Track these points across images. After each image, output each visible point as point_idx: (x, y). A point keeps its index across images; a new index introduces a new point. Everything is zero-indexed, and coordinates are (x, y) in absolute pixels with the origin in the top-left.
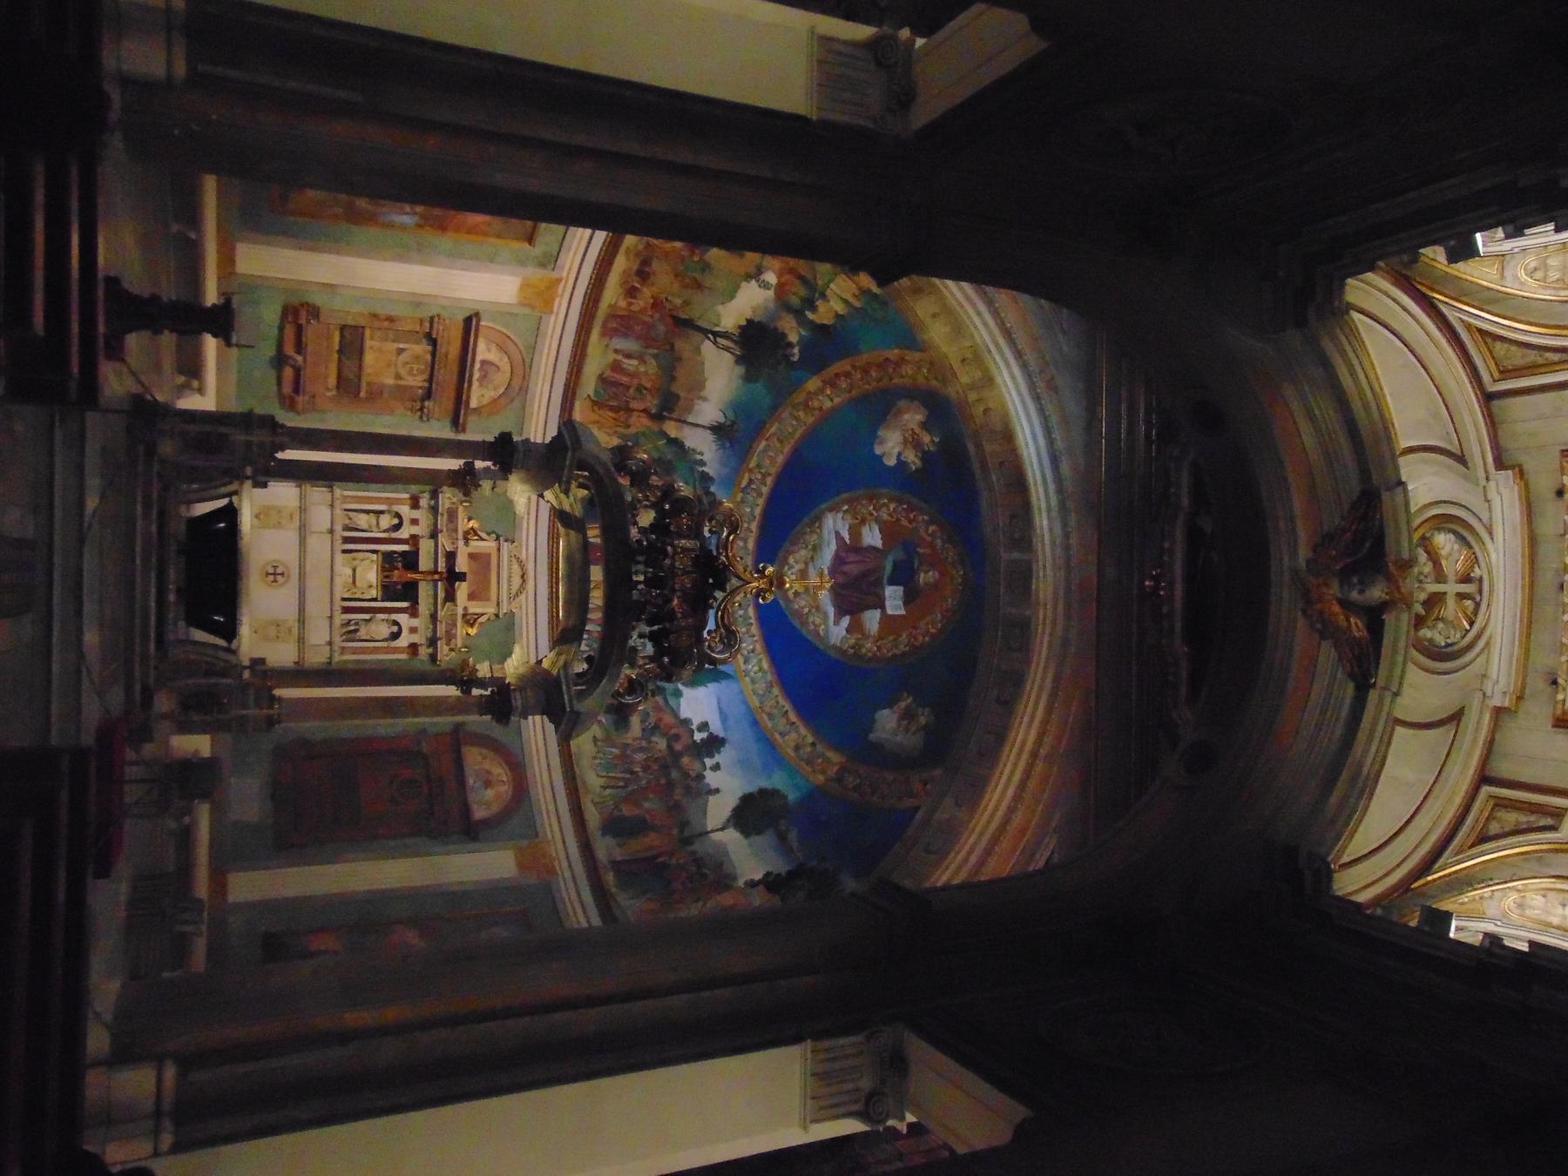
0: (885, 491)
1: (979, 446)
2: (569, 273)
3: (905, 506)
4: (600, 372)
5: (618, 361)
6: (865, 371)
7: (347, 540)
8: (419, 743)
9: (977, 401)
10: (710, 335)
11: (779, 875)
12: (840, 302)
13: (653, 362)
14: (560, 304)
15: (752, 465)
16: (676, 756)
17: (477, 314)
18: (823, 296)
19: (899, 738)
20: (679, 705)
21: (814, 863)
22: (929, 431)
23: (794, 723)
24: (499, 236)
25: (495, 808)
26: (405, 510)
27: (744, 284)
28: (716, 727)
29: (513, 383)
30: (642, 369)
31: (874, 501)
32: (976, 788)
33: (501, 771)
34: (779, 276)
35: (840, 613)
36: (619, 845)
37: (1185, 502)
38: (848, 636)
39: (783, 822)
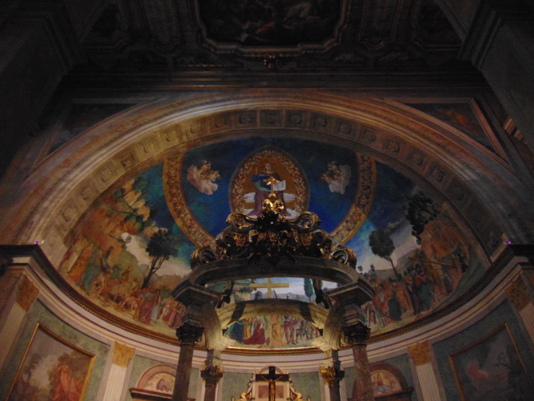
0: (229, 191)
1: (208, 138)
2: (113, 338)
3: (236, 180)
4: (168, 327)
5: (163, 318)
6: (173, 195)
9: (187, 136)
10: (154, 270)
11: (413, 228)
12: (138, 203)
13: (165, 300)
14: (130, 344)
17: (130, 390)
18: (135, 210)
19: (343, 178)
21: (406, 211)
22: (202, 164)
23: (337, 233)
24: (85, 374)
25: (393, 378)
27: (128, 250)
30: (168, 306)
31: (234, 196)
32: (366, 129)
34: (125, 231)
36: (405, 310)
37: (233, 46)
38: (296, 209)
39: (385, 232)
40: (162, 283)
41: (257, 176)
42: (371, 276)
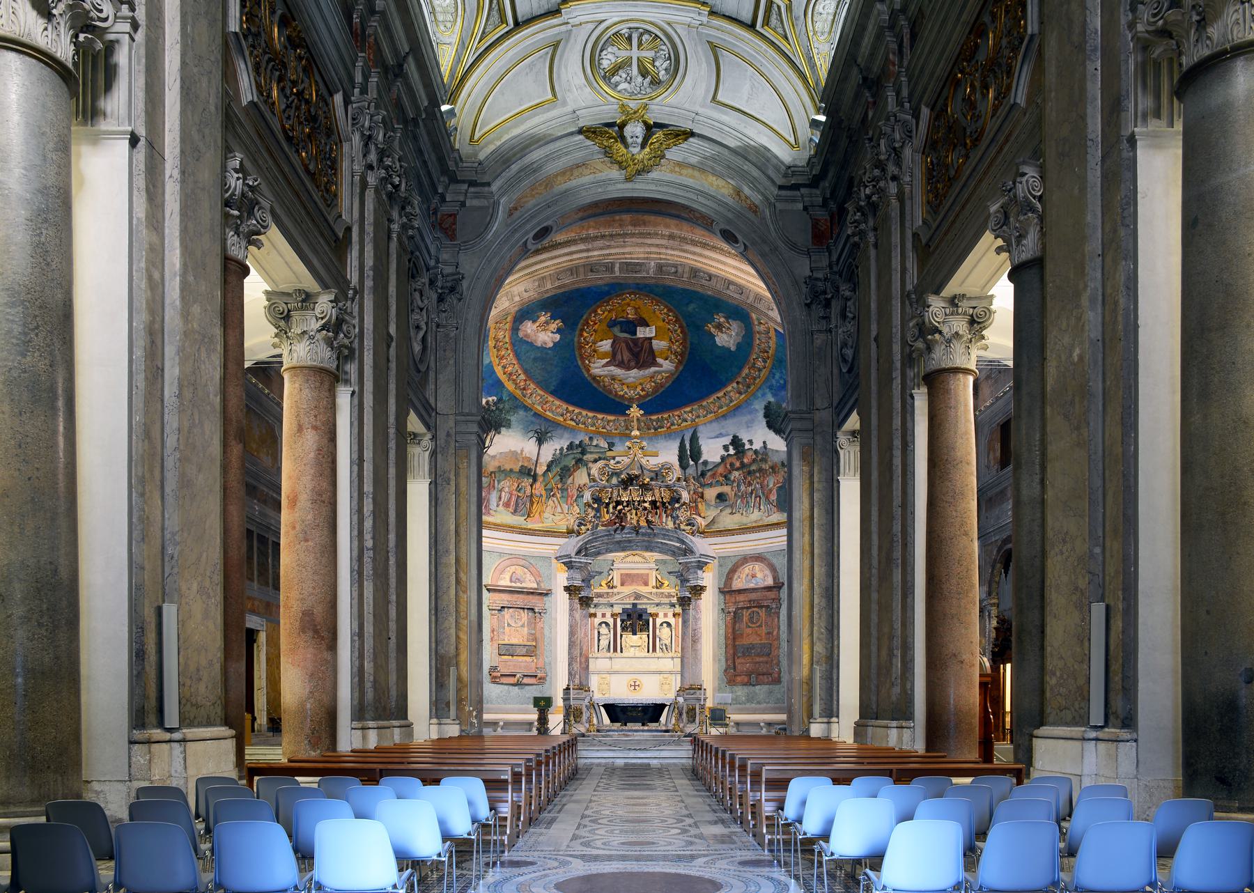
0: (576, 339)
1: (547, 291)
7: (615, 650)
8: (729, 612)
15: (561, 419)
16: (743, 465)
19: (734, 334)
20: (714, 462)
22: (538, 317)
25: (768, 572)
26: (597, 621)
28: (727, 440)
29: (521, 564)
30: (507, 489)
33: (746, 569)
35: (655, 364)
40: (497, 464)
41: (615, 320)
42: (762, 454)
